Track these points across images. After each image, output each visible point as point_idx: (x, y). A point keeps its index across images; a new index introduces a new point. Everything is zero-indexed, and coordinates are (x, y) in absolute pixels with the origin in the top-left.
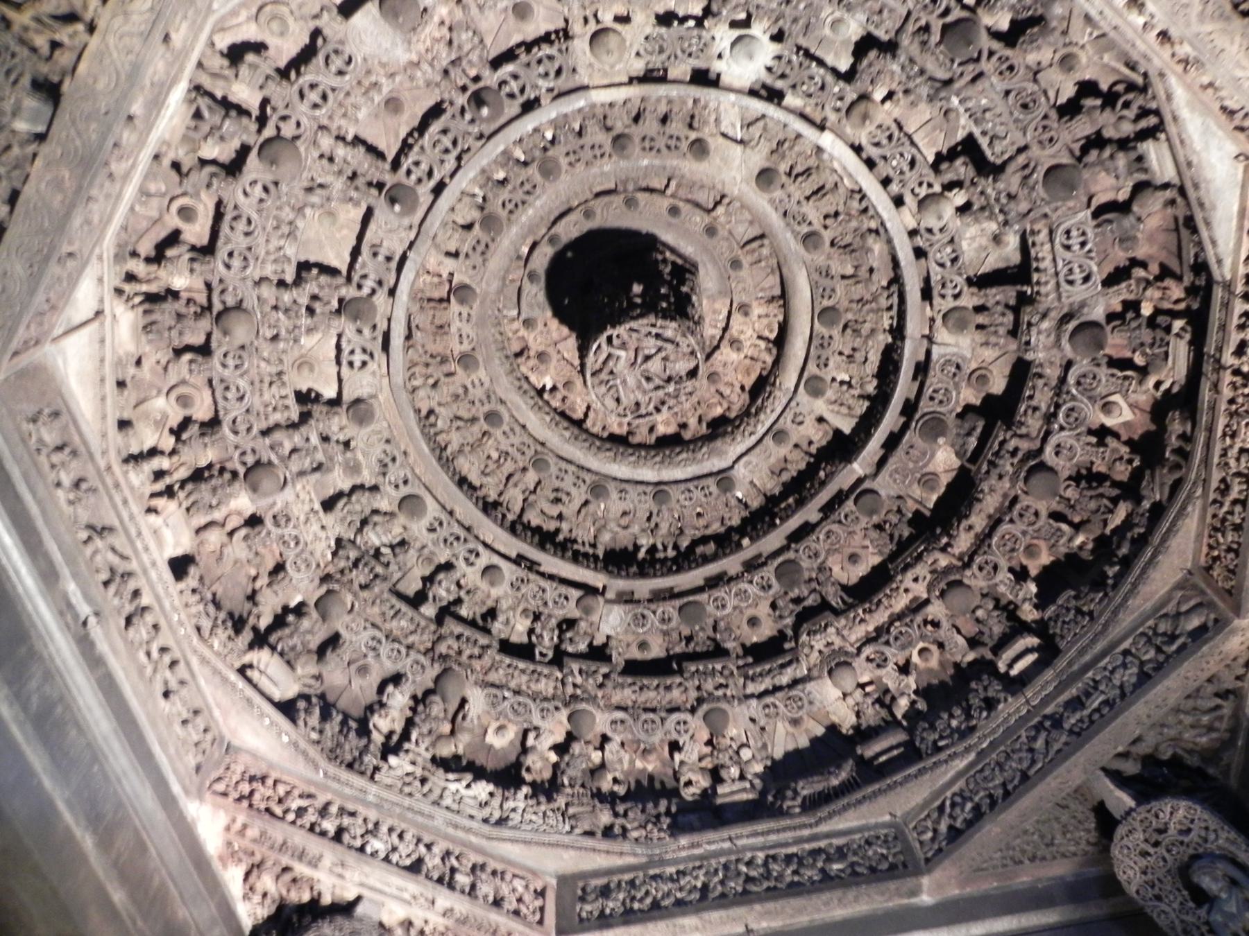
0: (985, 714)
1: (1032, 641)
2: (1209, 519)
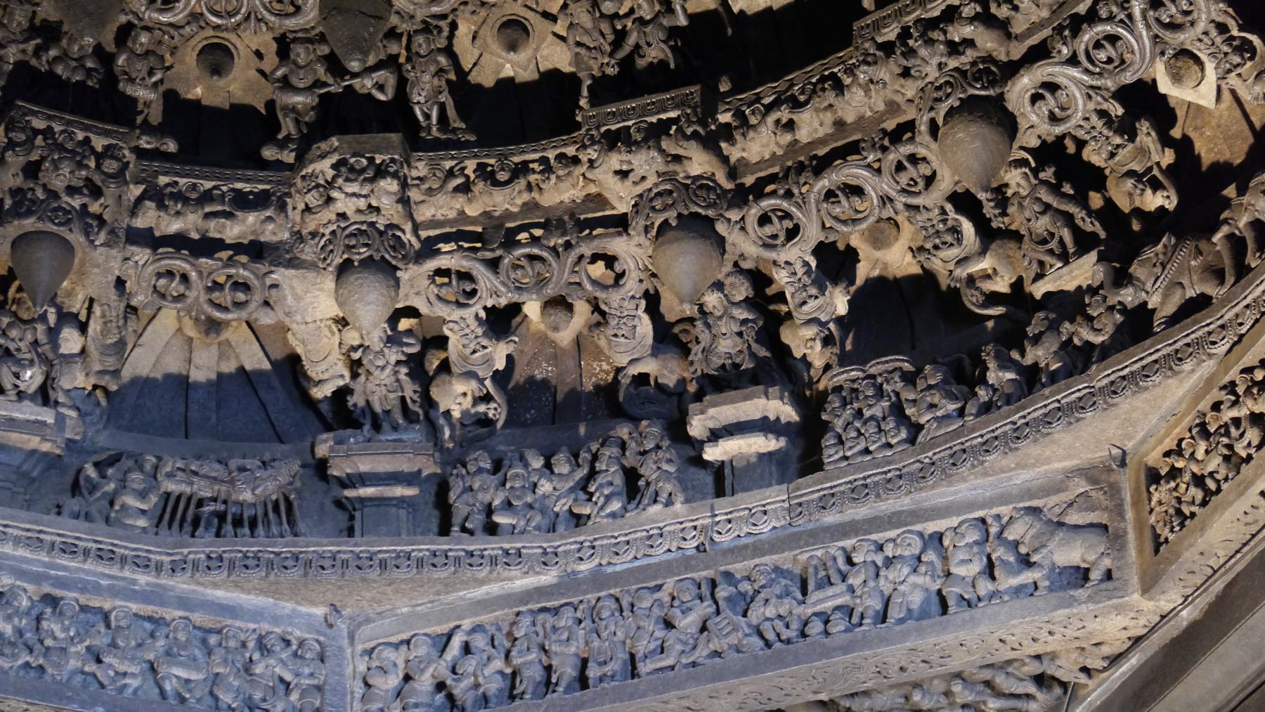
0: (616, 505)
1: (785, 411)
2: (1205, 405)
